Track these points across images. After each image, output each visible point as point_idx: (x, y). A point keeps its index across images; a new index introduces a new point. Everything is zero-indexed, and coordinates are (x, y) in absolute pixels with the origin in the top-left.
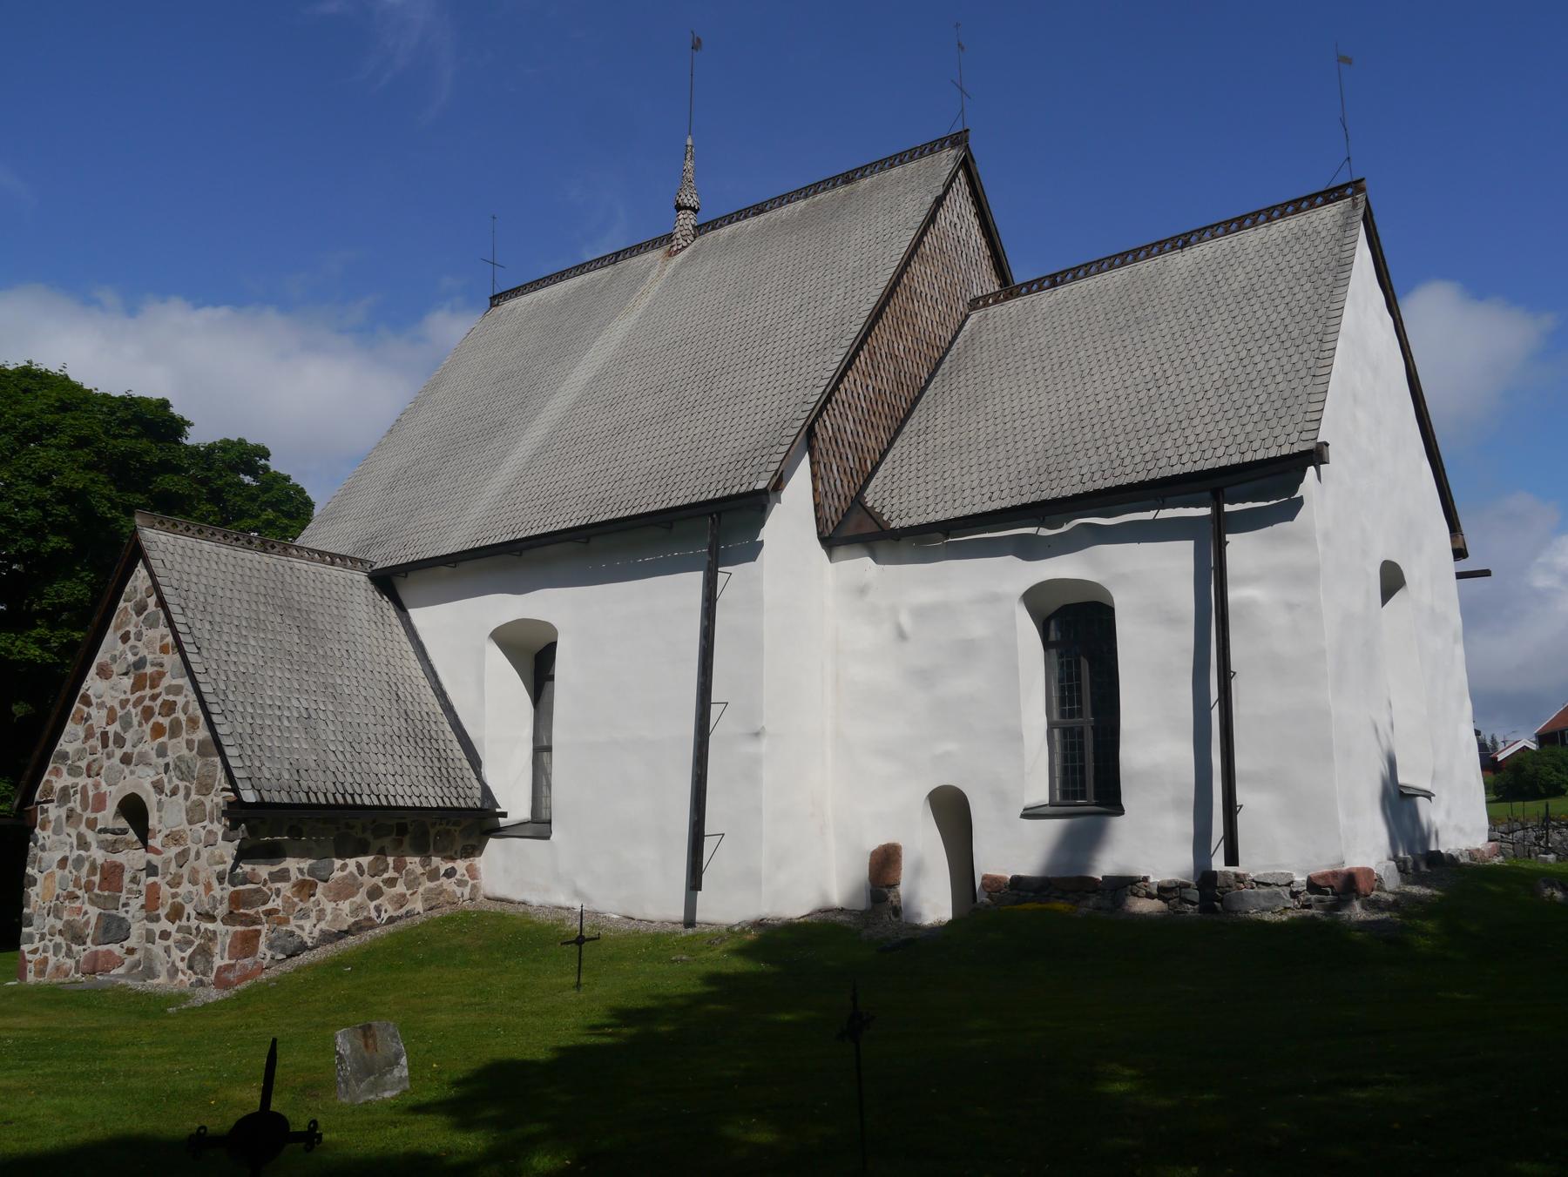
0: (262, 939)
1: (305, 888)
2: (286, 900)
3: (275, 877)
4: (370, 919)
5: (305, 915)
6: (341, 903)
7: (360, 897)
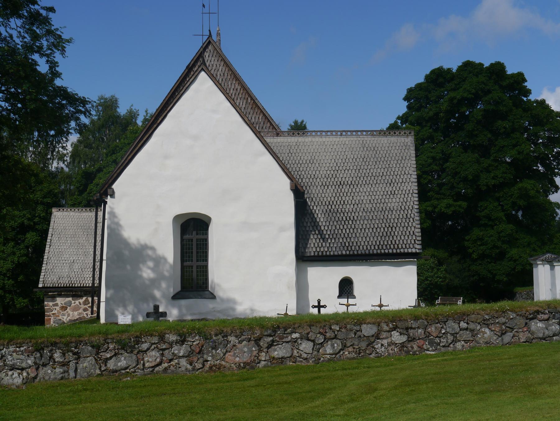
0: (52, 320)
1: (64, 308)
2: (58, 311)
3: (54, 305)
4: (84, 317)
5: (64, 315)
6: (74, 312)
7: (81, 311)
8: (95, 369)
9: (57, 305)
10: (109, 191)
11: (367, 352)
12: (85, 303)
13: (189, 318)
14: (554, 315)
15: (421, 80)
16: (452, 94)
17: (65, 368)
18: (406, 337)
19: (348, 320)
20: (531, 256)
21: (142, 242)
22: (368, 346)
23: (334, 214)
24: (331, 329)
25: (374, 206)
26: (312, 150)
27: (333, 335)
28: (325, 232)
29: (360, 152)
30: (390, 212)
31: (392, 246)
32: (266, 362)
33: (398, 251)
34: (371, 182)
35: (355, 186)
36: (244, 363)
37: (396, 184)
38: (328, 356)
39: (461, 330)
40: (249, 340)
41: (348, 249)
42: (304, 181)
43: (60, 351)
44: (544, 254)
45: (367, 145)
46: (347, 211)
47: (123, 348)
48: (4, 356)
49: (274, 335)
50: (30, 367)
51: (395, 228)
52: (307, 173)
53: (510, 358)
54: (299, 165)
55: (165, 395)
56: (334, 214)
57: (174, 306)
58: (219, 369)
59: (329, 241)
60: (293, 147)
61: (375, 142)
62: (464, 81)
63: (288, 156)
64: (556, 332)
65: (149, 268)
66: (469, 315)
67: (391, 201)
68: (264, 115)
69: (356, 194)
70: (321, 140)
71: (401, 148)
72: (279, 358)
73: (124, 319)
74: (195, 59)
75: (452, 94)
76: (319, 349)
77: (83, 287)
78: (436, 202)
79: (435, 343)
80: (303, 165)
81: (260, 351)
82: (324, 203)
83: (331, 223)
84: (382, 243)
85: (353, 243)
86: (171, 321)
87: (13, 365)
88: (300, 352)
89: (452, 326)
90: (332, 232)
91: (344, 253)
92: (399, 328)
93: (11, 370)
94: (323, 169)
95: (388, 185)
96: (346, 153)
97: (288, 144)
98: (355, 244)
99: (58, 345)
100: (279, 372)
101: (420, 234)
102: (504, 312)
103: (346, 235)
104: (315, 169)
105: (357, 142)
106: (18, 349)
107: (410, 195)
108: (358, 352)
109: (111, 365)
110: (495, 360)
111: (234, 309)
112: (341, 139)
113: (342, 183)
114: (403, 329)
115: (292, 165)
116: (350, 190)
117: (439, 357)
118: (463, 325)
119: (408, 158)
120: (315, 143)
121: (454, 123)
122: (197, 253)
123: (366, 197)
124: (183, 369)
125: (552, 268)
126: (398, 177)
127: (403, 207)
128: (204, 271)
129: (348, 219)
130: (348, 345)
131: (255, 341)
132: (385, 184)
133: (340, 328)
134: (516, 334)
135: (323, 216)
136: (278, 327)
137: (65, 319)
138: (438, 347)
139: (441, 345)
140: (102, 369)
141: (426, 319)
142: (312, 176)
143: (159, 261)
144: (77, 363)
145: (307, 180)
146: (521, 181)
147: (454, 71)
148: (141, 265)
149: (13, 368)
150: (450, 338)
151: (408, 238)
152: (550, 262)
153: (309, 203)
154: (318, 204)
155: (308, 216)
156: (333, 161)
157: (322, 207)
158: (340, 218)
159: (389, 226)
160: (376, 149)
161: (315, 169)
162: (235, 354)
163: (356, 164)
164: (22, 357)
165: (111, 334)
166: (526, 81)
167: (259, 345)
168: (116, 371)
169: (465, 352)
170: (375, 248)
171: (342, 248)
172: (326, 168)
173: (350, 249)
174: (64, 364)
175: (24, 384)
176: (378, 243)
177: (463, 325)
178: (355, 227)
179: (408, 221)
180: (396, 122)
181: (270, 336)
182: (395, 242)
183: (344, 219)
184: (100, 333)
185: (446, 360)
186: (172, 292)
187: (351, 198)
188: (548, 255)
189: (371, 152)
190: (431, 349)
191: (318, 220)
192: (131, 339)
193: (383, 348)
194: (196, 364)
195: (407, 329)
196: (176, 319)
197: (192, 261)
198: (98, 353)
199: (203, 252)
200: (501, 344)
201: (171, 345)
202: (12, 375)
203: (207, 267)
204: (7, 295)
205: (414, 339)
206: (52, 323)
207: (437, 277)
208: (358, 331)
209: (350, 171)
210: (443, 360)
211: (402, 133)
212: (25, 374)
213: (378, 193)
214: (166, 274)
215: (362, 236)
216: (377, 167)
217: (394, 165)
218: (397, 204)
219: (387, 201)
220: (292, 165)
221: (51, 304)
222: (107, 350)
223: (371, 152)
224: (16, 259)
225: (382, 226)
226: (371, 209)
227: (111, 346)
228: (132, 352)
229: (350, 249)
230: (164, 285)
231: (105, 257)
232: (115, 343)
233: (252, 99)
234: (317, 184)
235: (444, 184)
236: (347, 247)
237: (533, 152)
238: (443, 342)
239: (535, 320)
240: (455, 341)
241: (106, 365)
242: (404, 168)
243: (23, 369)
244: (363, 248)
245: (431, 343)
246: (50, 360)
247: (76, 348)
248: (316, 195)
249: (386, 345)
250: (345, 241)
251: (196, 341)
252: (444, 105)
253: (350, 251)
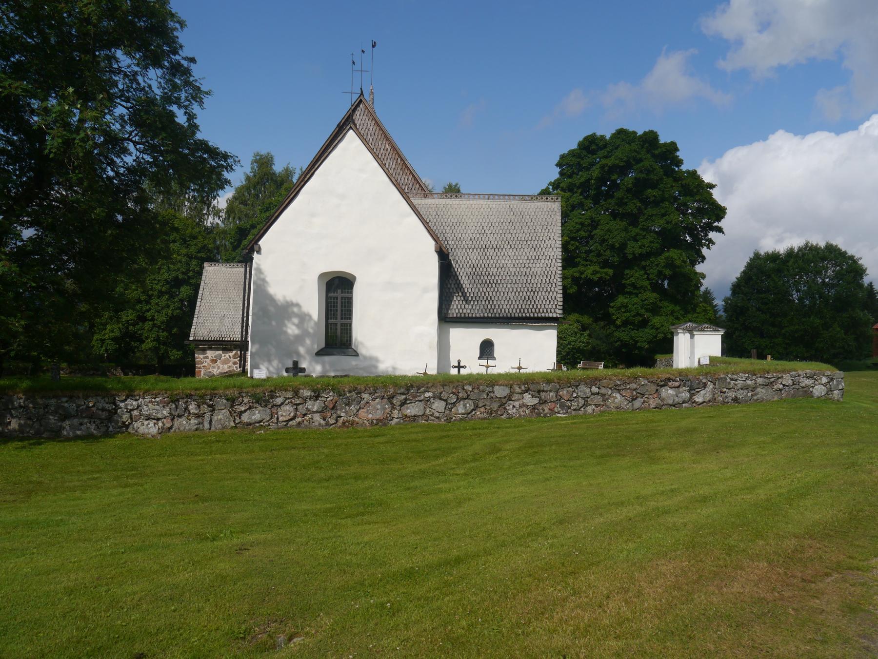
1: (214, 361)
5: (214, 367)
8: (229, 422)
9: (207, 358)
10: (256, 247)
11: (499, 413)
12: (234, 357)
13: (332, 374)
14: (685, 383)
15: (575, 146)
16: (604, 161)
17: (200, 420)
18: (538, 399)
19: (481, 381)
20: (673, 325)
21: (288, 299)
22: (500, 406)
23: (478, 277)
24: (464, 389)
25: (518, 270)
26: (459, 213)
27: (465, 395)
28: (468, 295)
29: (507, 217)
30: (533, 276)
31: (533, 311)
32: (398, 420)
33: (539, 315)
34: (516, 246)
35: (500, 250)
36: (377, 420)
37: (540, 249)
38: (460, 416)
39: (592, 395)
40: (383, 398)
41: (490, 312)
42: (450, 243)
43: (195, 403)
44: (686, 322)
45: (513, 210)
46: (491, 274)
47: (257, 402)
48: (140, 406)
49: (408, 394)
50: (165, 418)
51: (538, 292)
52: (453, 236)
53: (637, 424)
54: (446, 228)
55: (294, 448)
56: (478, 277)
57: (317, 362)
58: (352, 424)
59: (472, 303)
60: (440, 209)
61: (522, 206)
62: (617, 148)
63: (435, 218)
65: (294, 324)
66: (601, 380)
67: (534, 266)
68: (414, 176)
69: (501, 258)
70: (468, 202)
71: (547, 213)
72: (412, 416)
73: (260, 374)
74: (346, 117)
75: (604, 161)
76: (452, 408)
77: (233, 341)
78: (582, 269)
79: (566, 406)
80: (449, 227)
81: (393, 408)
82: (468, 266)
83: (475, 286)
84: (524, 307)
85: (495, 305)
86: (314, 376)
87: (149, 415)
88: (433, 411)
89: (584, 390)
90: (476, 295)
91: (486, 315)
92: (531, 390)
93: (147, 420)
94: (469, 232)
95: (533, 249)
96: (493, 217)
97: (435, 206)
98: (497, 307)
99: (193, 397)
100: (410, 430)
101: (562, 299)
102: (635, 378)
103: (489, 298)
104: (462, 231)
105: (504, 206)
106: (153, 400)
107: (554, 260)
108: (489, 412)
109: (245, 418)
110: (623, 425)
111: (376, 367)
112: (489, 203)
113: (487, 247)
114: (535, 391)
115: (439, 227)
116: (495, 253)
117: (569, 420)
118: (595, 389)
119: (554, 223)
120: (463, 206)
121: (606, 191)
122: (342, 311)
123: (510, 261)
124: (316, 424)
125: (692, 336)
126: (543, 242)
127: (546, 272)
128: (347, 329)
129: (492, 282)
130: (480, 406)
131: (389, 398)
132: (529, 249)
133: (473, 389)
134: (646, 400)
135: (467, 278)
136: (412, 386)
137: (216, 371)
138: (569, 410)
139: (572, 408)
140: (237, 422)
141: (558, 383)
142: (458, 239)
143: (304, 317)
144: (212, 415)
145: (453, 242)
146: (668, 251)
147: (608, 138)
148: (286, 322)
149: (148, 418)
150: (581, 402)
151: (550, 302)
152: (691, 331)
153: (454, 265)
154: (463, 266)
155: (452, 278)
156: (479, 224)
157: (467, 269)
158: (484, 281)
159: (532, 290)
160: (522, 213)
161: (462, 231)
162: (368, 410)
163: (502, 228)
164: (157, 407)
165: (245, 388)
166: (679, 151)
167: (392, 403)
168: (250, 424)
169: (595, 416)
170: (516, 311)
171: (484, 310)
172: (472, 231)
173: (492, 312)
174: (199, 416)
175: (160, 433)
176: (520, 307)
177: (595, 389)
178: (498, 290)
179: (550, 286)
180: (547, 188)
181: (403, 394)
182: (537, 306)
183: (488, 282)
184: (234, 387)
185: (575, 423)
186: (316, 348)
187: (495, 262)
188: (689, 324)
189: (517, 217)
190: (561, 412)
191: (462, 282)
192: (265, 394)
193: (515, 409)
194: (329, 420)
195: (539, 392)
196: (319, 375)
197: (336, 319)
198: (232, 406)
199: (348, 310)
200: (631, 409)
201: (305, 400)
202: (147, 425)
203: (350, 325)
204: (162, 347)
205: (546, 401)
206: (202, 375)
207: (580, 342)
208: (490, 392)
209: (496, 235)
210: (572, 423)
211: (549, 198)
212: (160, 424)
213: (523, 257)
214: (311, 331)
215: (504, 299)
216: (522, 231)
217: (540, 230)
218: (540, 269)
219: (531, 266)
220: (439, 227)
221: (201, 356)
222: (241, 403)
223: (517, 217)
224: (170, 312)
225: (524, 290)
226: (515, 273)
227: (246, 400)
228: (266, 406)
229: (492, 312)
230: (308, 342)
231: (250, 313)
232: (250, 396)
233: (402, 160)
234: (462, 246)
235: (590, 251)
236: (490, 310)
237: (682, 222)
238: (574, 406)
240: (586, 405)
241: (240, 418)
242: (549, 234)
243: (158, 419)
244: (505, 311)
245: (562, 406)
246: (185, 411)
247: (211, 400)
248: (461, 258)
249: (518, 406)
250: (487, 303)
251: (330, 397)
252: (595, 172)
253: (492, 314)
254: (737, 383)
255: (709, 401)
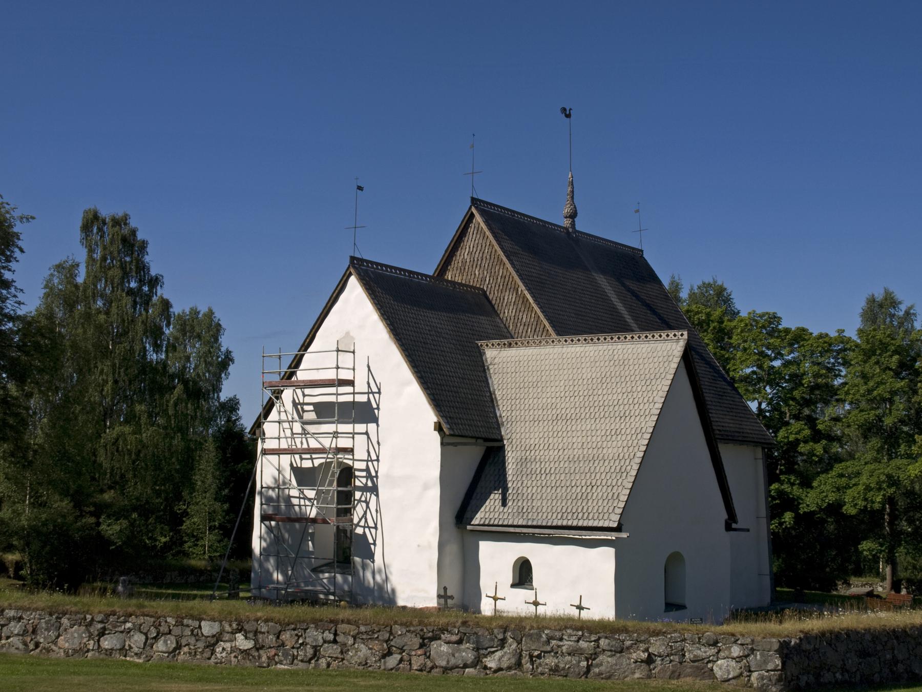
14: (469, 637)
64: (468, 662)
108: (193, 654)
139: (299, 658)
150: (310, 651)
190: (285, 662)
205: (263, 646)
239: (439, 642)
249: (229, 649)
254: (561, 643)
255: (509, 668)
